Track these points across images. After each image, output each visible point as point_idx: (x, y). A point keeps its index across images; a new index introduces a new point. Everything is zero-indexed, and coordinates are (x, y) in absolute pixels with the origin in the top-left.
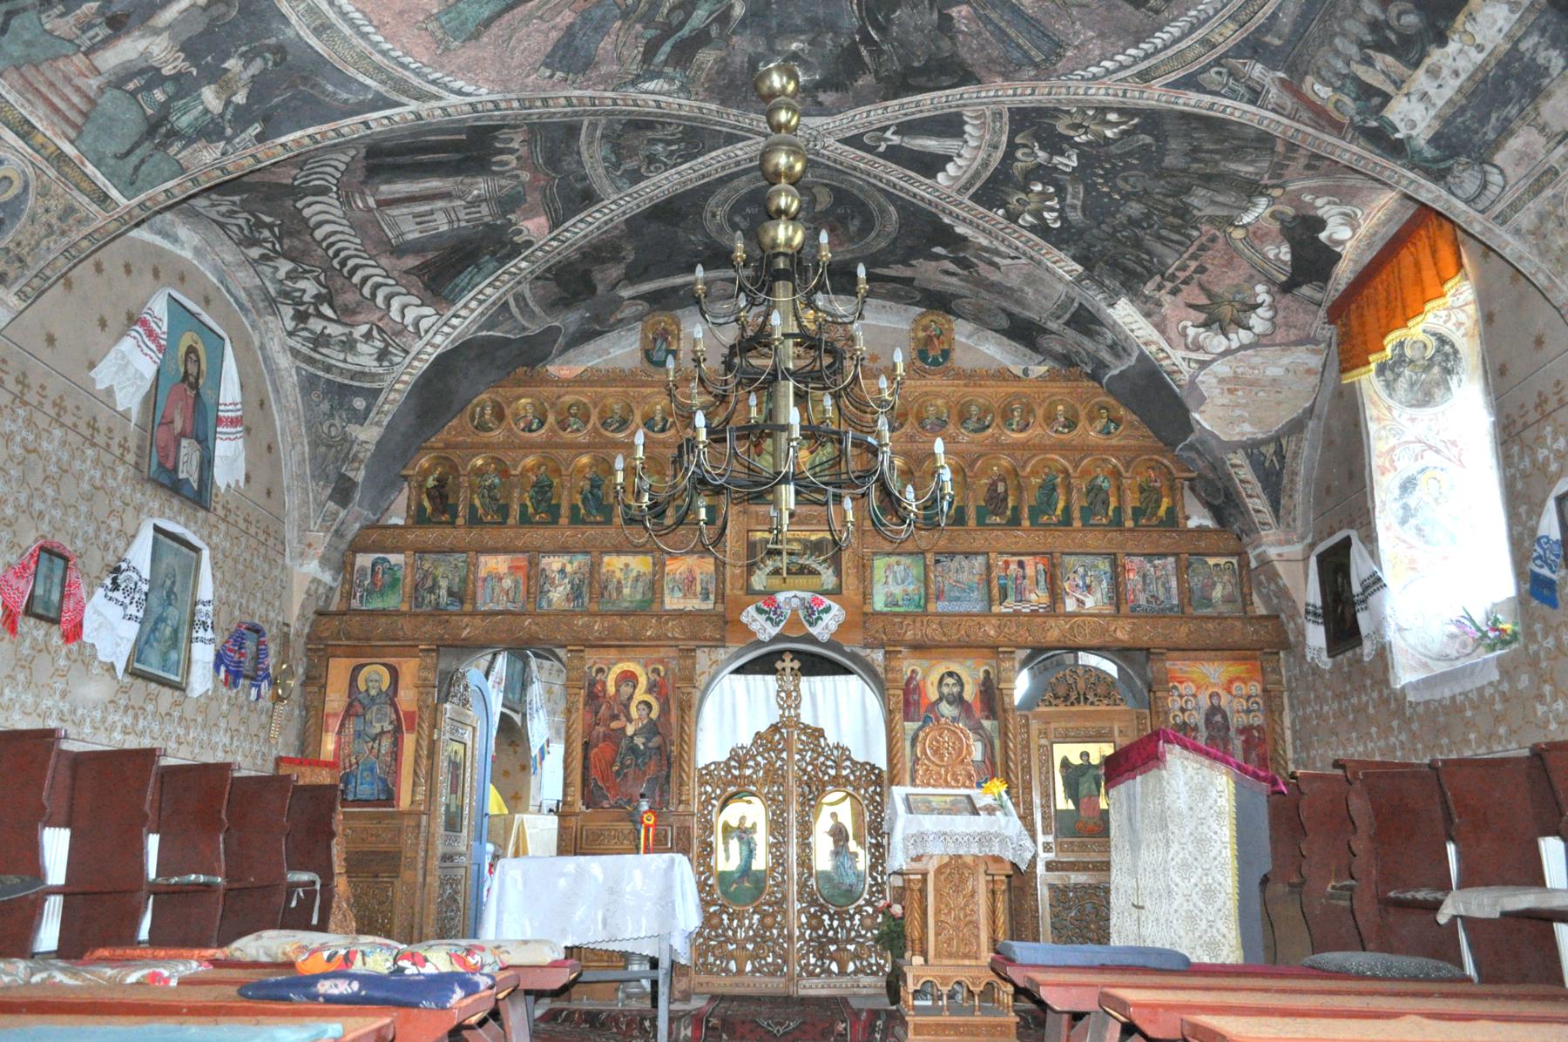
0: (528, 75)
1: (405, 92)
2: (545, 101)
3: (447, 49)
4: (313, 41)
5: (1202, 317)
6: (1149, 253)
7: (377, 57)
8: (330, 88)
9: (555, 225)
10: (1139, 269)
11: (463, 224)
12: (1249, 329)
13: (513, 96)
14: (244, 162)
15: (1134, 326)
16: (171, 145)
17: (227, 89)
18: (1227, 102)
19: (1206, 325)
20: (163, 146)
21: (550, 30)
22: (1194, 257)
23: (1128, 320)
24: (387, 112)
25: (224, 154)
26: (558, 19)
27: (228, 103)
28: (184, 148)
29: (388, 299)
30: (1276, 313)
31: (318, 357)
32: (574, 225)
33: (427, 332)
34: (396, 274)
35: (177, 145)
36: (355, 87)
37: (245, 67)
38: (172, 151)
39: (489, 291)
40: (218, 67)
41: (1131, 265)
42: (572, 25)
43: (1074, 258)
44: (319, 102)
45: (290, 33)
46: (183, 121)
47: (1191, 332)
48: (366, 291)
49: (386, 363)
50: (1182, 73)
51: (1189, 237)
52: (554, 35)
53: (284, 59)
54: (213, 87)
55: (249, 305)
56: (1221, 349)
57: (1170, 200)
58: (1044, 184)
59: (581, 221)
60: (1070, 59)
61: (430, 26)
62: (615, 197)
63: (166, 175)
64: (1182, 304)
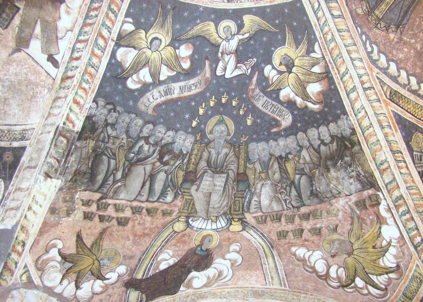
5: (73, 251)
6: (125, 176)
10: (100, 178)
12: (78, 287)
15: (35, 207)
18: (408, 159)
19: (65, 258)
22: (136, 211)
23: (40, 198)
30: (102, 293)
41: (103, 168)
43: (89, 118)
47: (54, 252)
50: (413, 120)
51: (163, 194)
56: (48, 284)
57: (203, 164)
58: (191, 58)
60: (387, 38)
64: (77, 229)
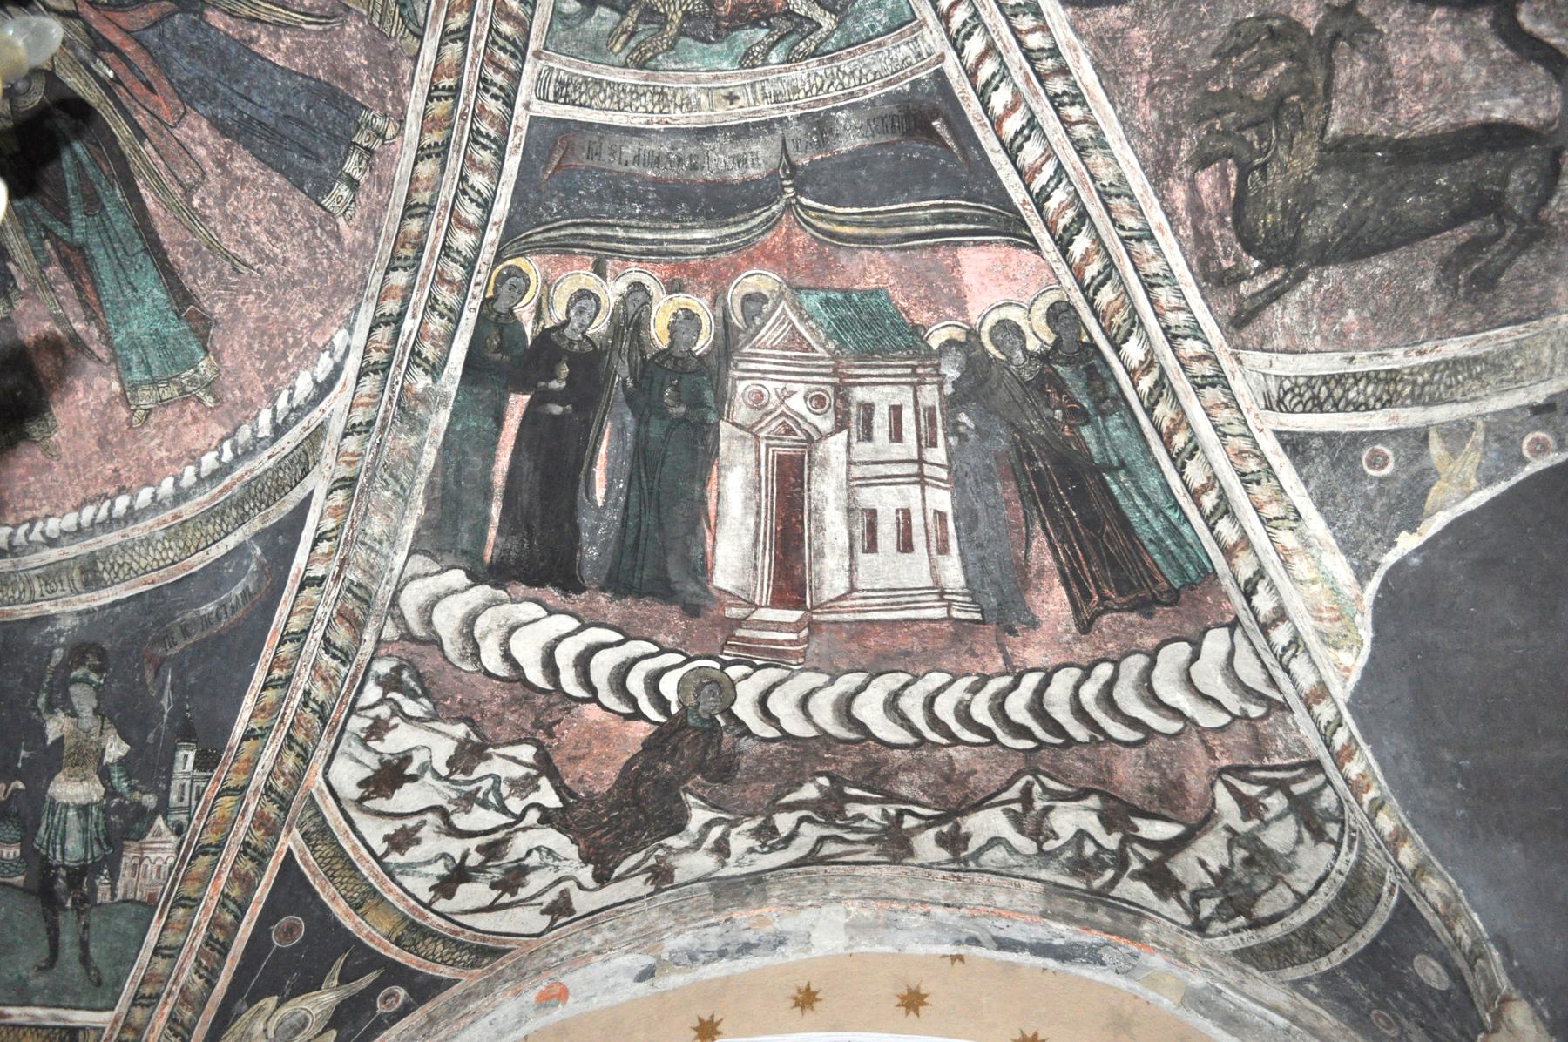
0: (338, 237)
1: (280, 490)
2: (409, 210)
3: (209, 386)
4: (107, 596)
7: (188, 509)
8: (209, 608)
9: (1011, 228)
11: (938, 454)
13: (375, 280)
14: (218, 812)
16: (94, 890)
17: (85, 757)
20: (85, 902)
21: (226, 172)
24: (307, 535)
25: (179, 830)
26: (201, 152)
27: (104, 774)
28: (114, 877)
29: (1155, 703)
31: (1275, 931)
32: (1026, 176)
33: (1272, 682)
34: (1083, 651)
35: (102, 883)
36: (229, 569)
37: (74, 714)
38: (103, 895)
39: (1196, 473)
40: (47, 750)
42: (218, 125)
44: (219, 638)
45: (67, 623)
46: (74, 847)
48: (1117, 730)
49: (1333, 830)
52: (243, 164)
53: (102, 654)
54: (60, 776)
55: (1092, 937)
59: (1012, 151)
61: (145, 403)
62: (933, 38)
63: (133, 931)
